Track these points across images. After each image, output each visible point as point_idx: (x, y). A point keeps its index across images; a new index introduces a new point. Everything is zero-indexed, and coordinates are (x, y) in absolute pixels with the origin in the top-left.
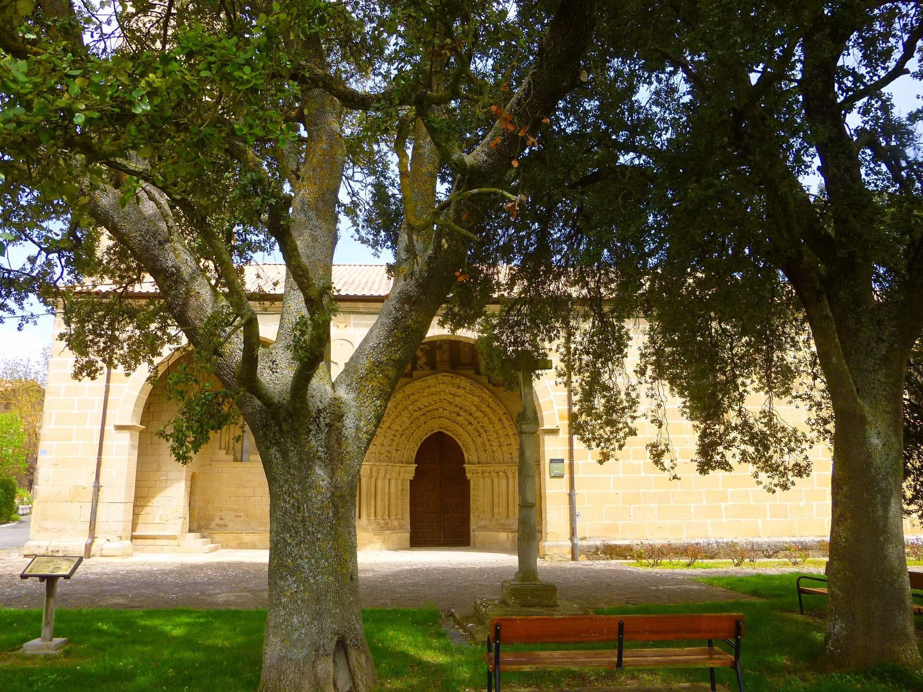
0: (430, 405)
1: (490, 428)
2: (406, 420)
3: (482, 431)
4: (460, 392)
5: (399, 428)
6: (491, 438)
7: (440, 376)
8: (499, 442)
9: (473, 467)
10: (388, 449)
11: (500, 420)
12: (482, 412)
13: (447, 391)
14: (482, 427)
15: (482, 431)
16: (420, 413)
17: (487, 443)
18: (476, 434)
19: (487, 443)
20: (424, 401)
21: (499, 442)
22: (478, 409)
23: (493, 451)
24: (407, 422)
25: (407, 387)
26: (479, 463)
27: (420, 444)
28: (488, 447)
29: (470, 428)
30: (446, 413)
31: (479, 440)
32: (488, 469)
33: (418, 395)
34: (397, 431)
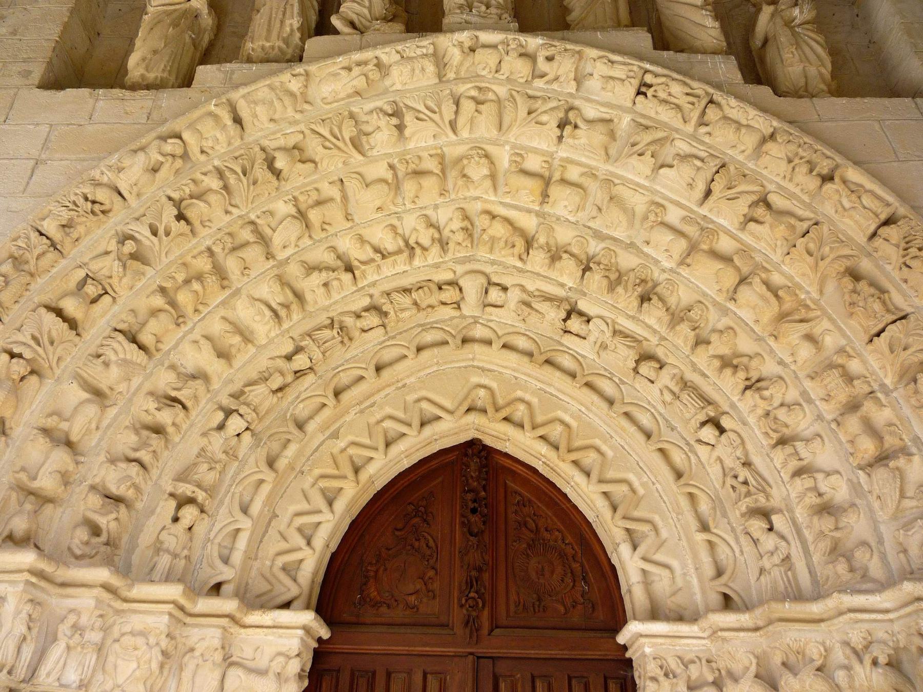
0: (410, 249)
1: (791, 352)
2: (263, 327)
3: (725, 388)
4: (581, 151)
5: (204, 359)
6: (800, 422)
7: (449, 44)
8: (870, 429)
9: (690, 639)
10: (114, 479)
11: (855, 275)
12: (726, 259)
13: (504, 158)
14: (727, 363)
15: (725, 388)
16: (346, 297)
17: (773, 465)
18: (690, 412)
19: (773, 465)
20: (371, 218)
21: (870, 429)
22: (698, 245)
23: (826, 509)
24: (271, 339)
25: (261, 90)
26: (727, 603)
27: (352, 496)
28: (785, 492)
29: (650, 393)
30: (505, 318)
31: (712, 460)
32: (810, 640)
33: (332, 164)
34: (200, 376)
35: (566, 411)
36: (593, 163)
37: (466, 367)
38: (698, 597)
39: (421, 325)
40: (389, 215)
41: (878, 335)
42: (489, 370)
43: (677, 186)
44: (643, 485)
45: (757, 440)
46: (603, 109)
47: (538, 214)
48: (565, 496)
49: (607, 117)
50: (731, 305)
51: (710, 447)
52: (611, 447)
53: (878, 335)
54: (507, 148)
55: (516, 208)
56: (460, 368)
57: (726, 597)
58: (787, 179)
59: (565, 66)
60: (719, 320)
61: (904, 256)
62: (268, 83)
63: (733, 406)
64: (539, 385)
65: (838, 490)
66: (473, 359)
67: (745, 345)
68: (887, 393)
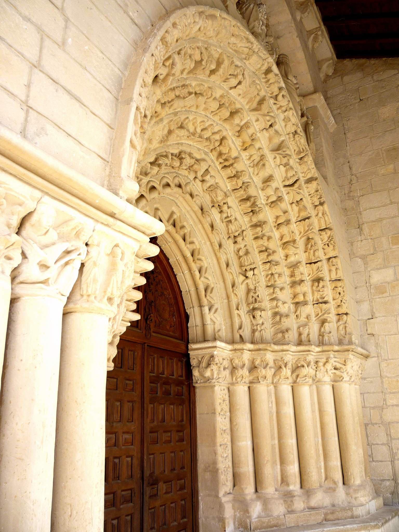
6: (279, 282)
35: (197, 239)
36: (264, 146)
37: (172, 200)
38: (224, 334)
39: (177, 173)
40: (206, 116)
41: (315, 263)
42: (179, 207)
43: (279, 174)
44: (214, 283)
45: (263, 282)
46: (280, 129)
47: (239, 153)
48: (175, 276)
49: (280, 133)
50: (274, 229)
51: (245, 278)
52: (207, 262)
53: (315, 263)
54: (249, 118)
55: (234, 144)
56: (170, 199)
57: (241, 336)
58: (311, 196)
59: (283, 102)
60: (268, 232)
61: (329, 242)
62: (231, 20)
63: (259, 266)
64: (192, 223)
65: (283, 309)
66: (177, 198)
67: (272, 245)
68: (307, 282)
